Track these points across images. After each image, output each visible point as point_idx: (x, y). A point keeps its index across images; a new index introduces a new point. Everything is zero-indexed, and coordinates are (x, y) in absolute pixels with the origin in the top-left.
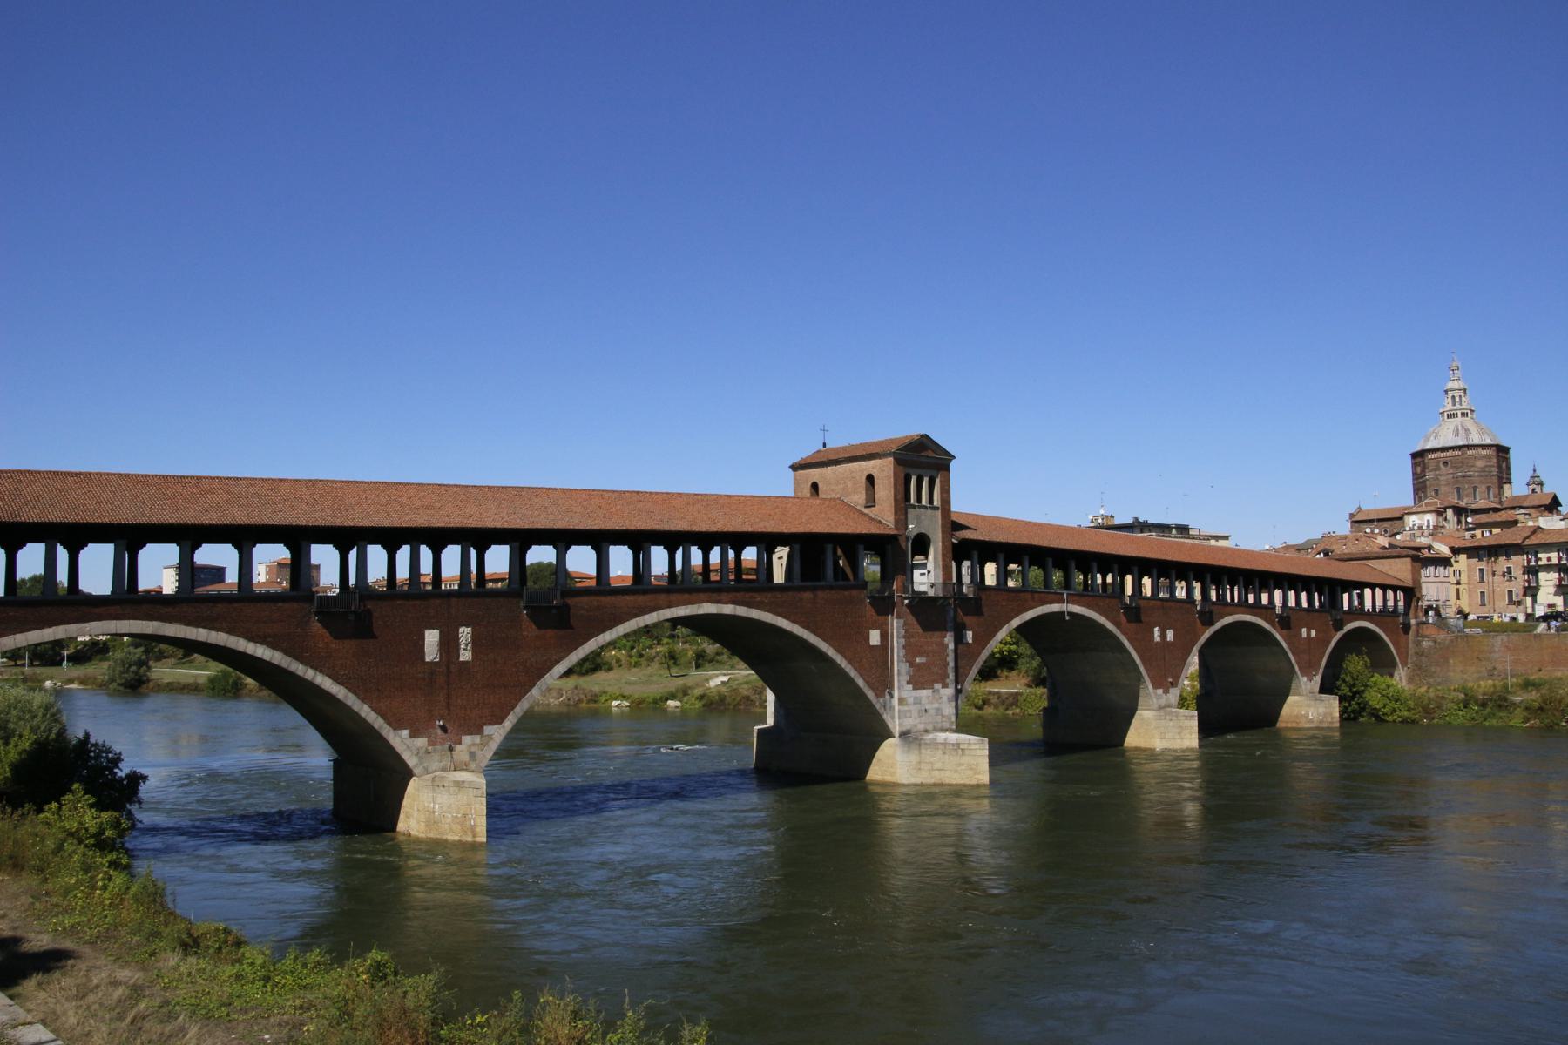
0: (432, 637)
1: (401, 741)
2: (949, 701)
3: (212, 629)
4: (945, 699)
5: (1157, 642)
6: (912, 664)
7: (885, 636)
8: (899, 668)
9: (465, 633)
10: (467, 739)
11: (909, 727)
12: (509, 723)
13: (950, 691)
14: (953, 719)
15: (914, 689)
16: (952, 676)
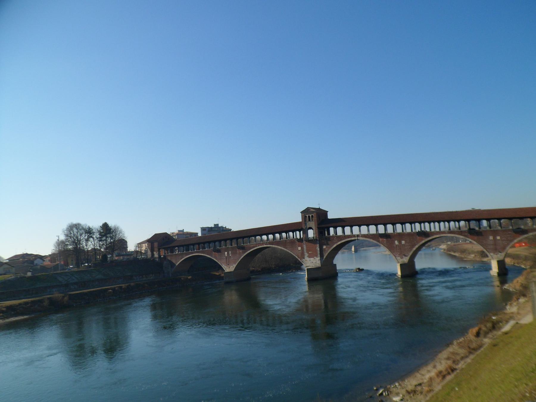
0: (226, 253)
1: (224, 267)
2: (318, 260)
3: (204, 254)
4: (317, 260)
5: (397, 245)
6: (308, 253)
7: (301, 248)
8: (306, 255)
9: (230, 252)
10: (231, 266)
11: (308, 266)
12: (236, 265)
13: (319, 258)
14: (320, 264)
15: (309, 258)
16: (319, 255)
